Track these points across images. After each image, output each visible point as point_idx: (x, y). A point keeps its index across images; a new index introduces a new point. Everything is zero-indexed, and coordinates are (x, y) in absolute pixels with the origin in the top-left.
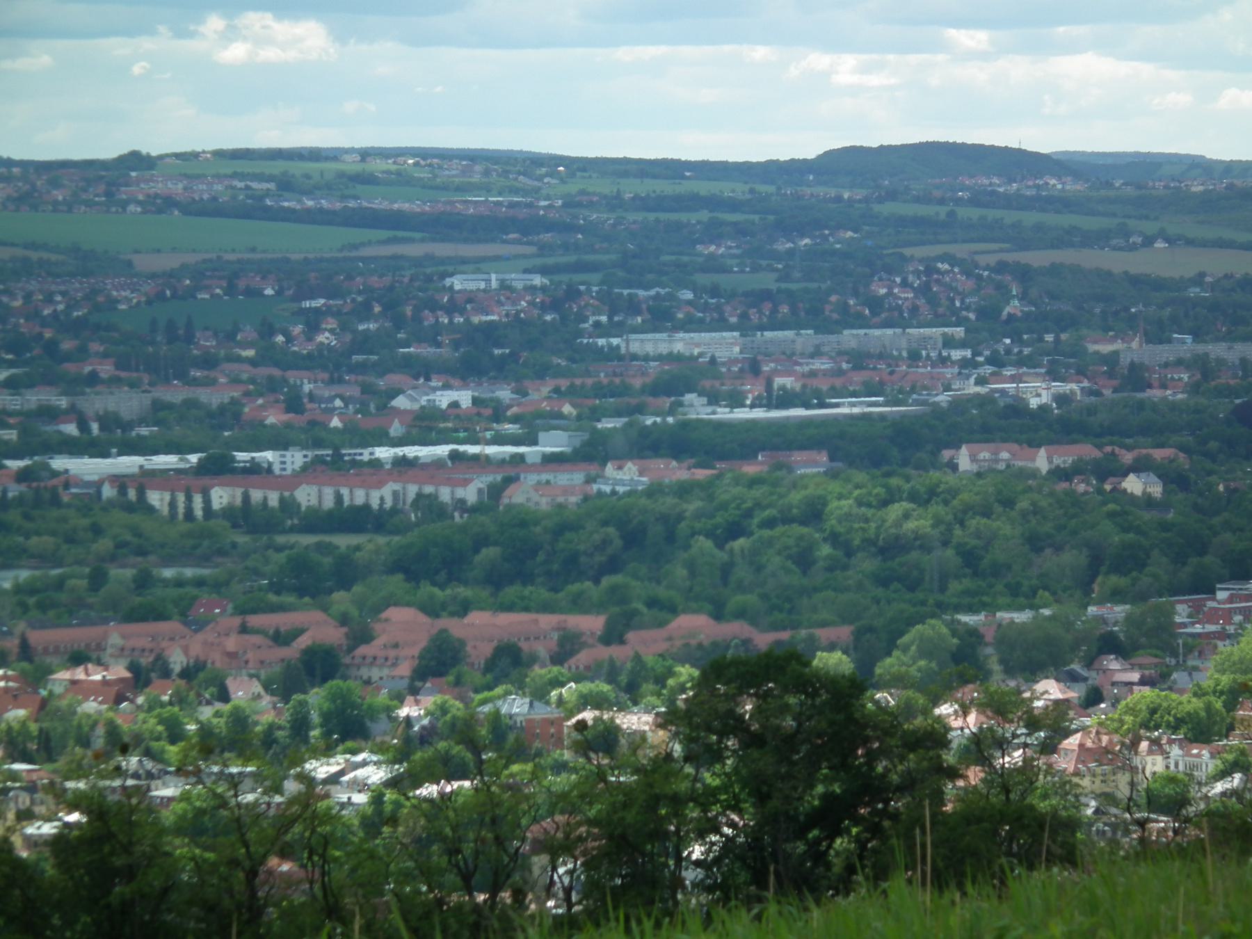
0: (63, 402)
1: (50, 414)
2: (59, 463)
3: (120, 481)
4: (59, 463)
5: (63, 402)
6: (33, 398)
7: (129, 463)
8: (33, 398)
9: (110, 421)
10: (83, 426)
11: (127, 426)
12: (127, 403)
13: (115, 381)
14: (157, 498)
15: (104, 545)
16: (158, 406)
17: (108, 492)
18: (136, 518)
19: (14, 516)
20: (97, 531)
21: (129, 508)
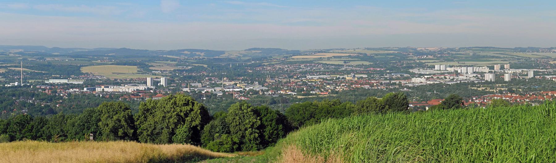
0: (545, 71)
1: (544, 72)
2: (545, 76)
3: (551, 78)
4: (545, 76)
5: (545, 71)
6: (543, 70)
7: (551, 76)
8: (543, 70)
9: (550, 72)
10: (548, 73)
11: (551, 73)
12: (551, 70)
13: (550, 69)
14: (554, 80)
15: (549, 84)
16: (554, 71)
17: (549, 79)
18: (552, 81)
19: (542, 81)
20: (549, 82)
21: (552, 80)
